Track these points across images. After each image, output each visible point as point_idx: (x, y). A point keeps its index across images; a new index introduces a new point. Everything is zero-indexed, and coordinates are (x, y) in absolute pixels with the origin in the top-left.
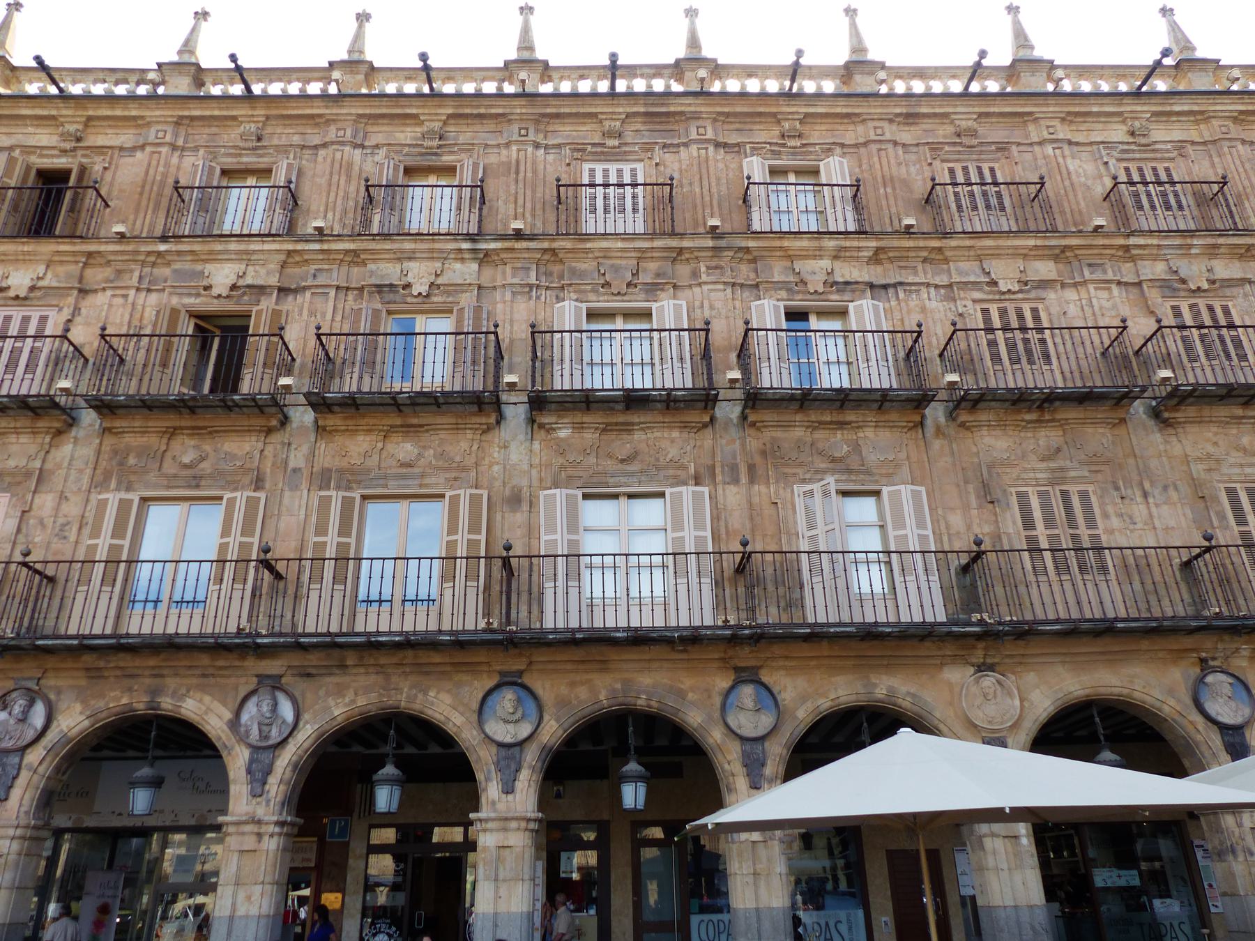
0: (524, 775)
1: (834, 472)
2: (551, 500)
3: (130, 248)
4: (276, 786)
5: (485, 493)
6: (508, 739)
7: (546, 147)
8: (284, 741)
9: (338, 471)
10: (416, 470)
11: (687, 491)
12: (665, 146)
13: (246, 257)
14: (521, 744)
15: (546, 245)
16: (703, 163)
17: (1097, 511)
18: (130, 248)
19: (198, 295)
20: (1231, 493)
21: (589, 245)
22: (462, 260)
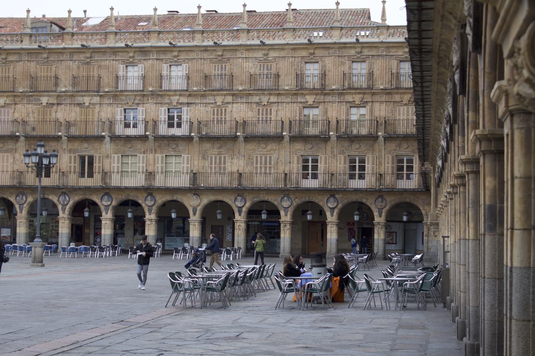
0: (109, 211)
1: (172, 151)
2: (114, 157)
3: (24, 94)
4: (67, 212)
5: (101, 155)
6: (106, 205)
7: (116, 60)
8: (67, 204)
9: (73, 150)
10: (88, 150)
11: (141, 156)
12: (144, 59)
13: (49, 96)
14: (109, 205)
15: (114, 93)
16: (153, 65)
17: (227, 161)
18: (24, 94)
19: (40, 105)
20: (257, 157)
21: (123, 93)
22: (96, 96)
